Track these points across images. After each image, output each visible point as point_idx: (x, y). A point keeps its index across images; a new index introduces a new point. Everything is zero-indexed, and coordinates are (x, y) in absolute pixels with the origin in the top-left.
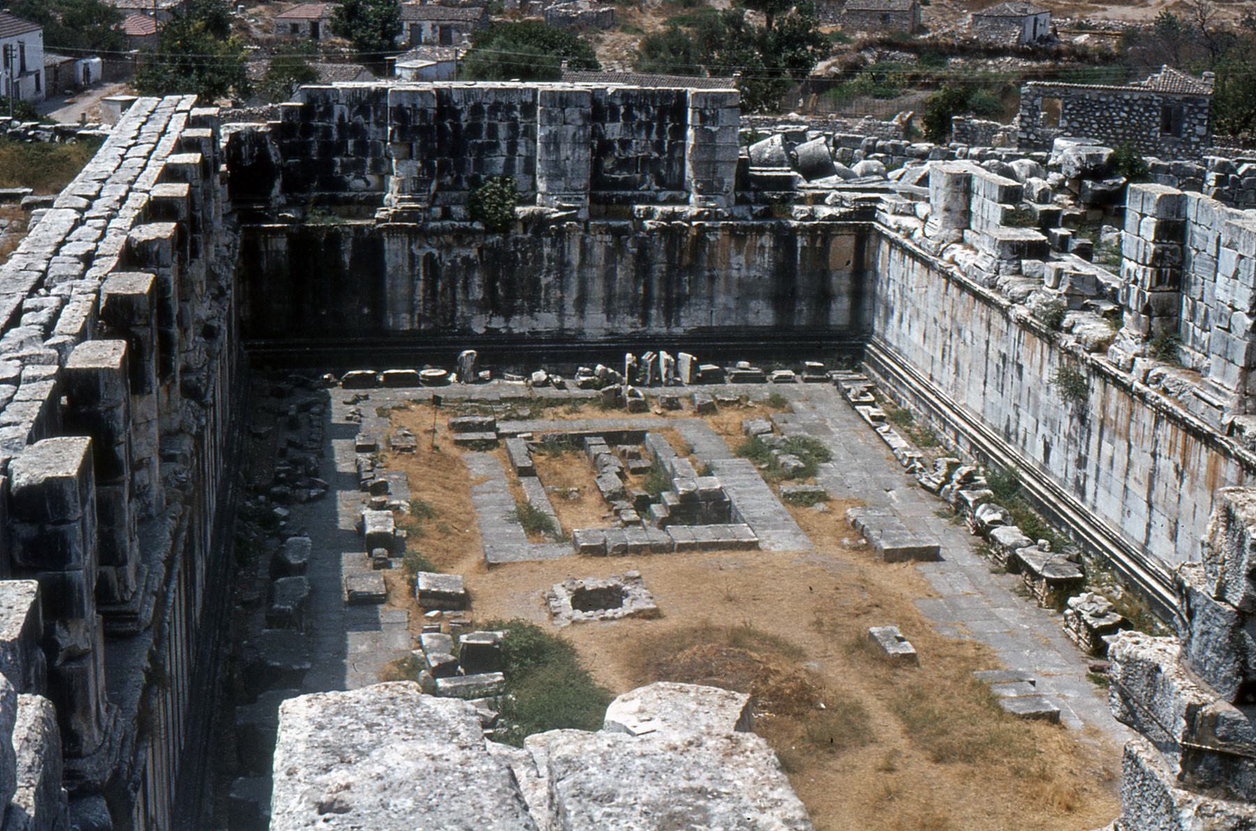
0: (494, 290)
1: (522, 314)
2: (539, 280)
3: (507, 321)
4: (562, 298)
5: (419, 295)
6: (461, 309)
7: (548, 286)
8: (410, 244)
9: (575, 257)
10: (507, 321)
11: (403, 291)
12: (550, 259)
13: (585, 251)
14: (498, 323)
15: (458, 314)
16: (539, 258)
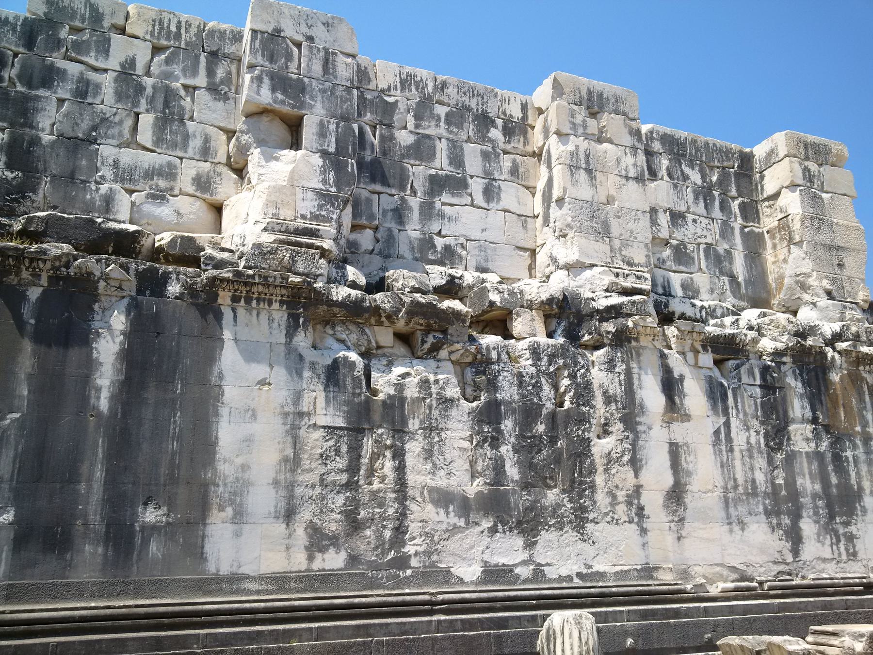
0: (498, 468)
1: (560, 526)
2: (586, 443)
3: (530, 545)
4: (638, 490)
5: (310, 474)
6: (423, 514)
7: (610, 460)
8: (292, 329)
9: (651, 394)
10: (530, 545)
11: (266, 459)
12: (609, 399)
13: (671, 386)
14: (508, 550)
15: (414, 527)
16: (583, 392)
